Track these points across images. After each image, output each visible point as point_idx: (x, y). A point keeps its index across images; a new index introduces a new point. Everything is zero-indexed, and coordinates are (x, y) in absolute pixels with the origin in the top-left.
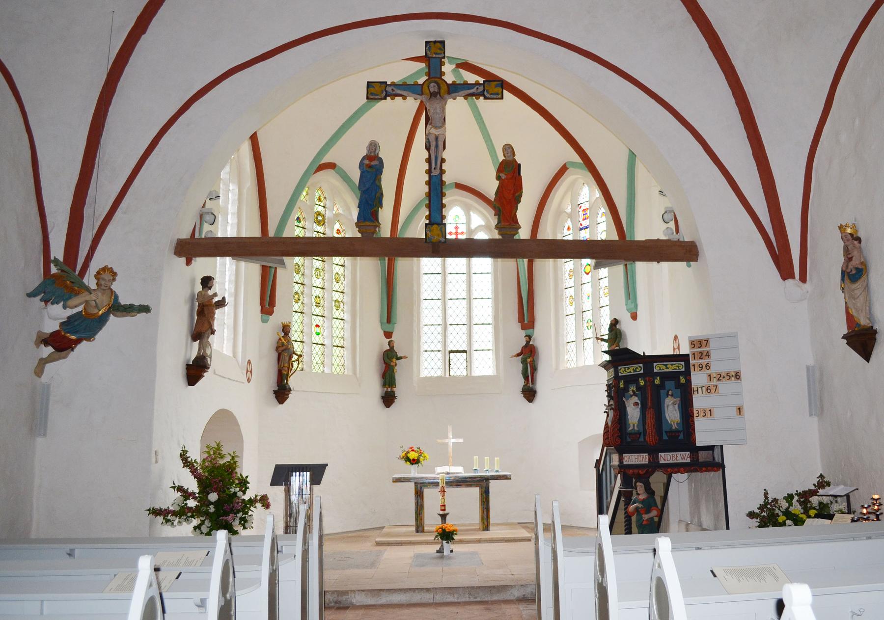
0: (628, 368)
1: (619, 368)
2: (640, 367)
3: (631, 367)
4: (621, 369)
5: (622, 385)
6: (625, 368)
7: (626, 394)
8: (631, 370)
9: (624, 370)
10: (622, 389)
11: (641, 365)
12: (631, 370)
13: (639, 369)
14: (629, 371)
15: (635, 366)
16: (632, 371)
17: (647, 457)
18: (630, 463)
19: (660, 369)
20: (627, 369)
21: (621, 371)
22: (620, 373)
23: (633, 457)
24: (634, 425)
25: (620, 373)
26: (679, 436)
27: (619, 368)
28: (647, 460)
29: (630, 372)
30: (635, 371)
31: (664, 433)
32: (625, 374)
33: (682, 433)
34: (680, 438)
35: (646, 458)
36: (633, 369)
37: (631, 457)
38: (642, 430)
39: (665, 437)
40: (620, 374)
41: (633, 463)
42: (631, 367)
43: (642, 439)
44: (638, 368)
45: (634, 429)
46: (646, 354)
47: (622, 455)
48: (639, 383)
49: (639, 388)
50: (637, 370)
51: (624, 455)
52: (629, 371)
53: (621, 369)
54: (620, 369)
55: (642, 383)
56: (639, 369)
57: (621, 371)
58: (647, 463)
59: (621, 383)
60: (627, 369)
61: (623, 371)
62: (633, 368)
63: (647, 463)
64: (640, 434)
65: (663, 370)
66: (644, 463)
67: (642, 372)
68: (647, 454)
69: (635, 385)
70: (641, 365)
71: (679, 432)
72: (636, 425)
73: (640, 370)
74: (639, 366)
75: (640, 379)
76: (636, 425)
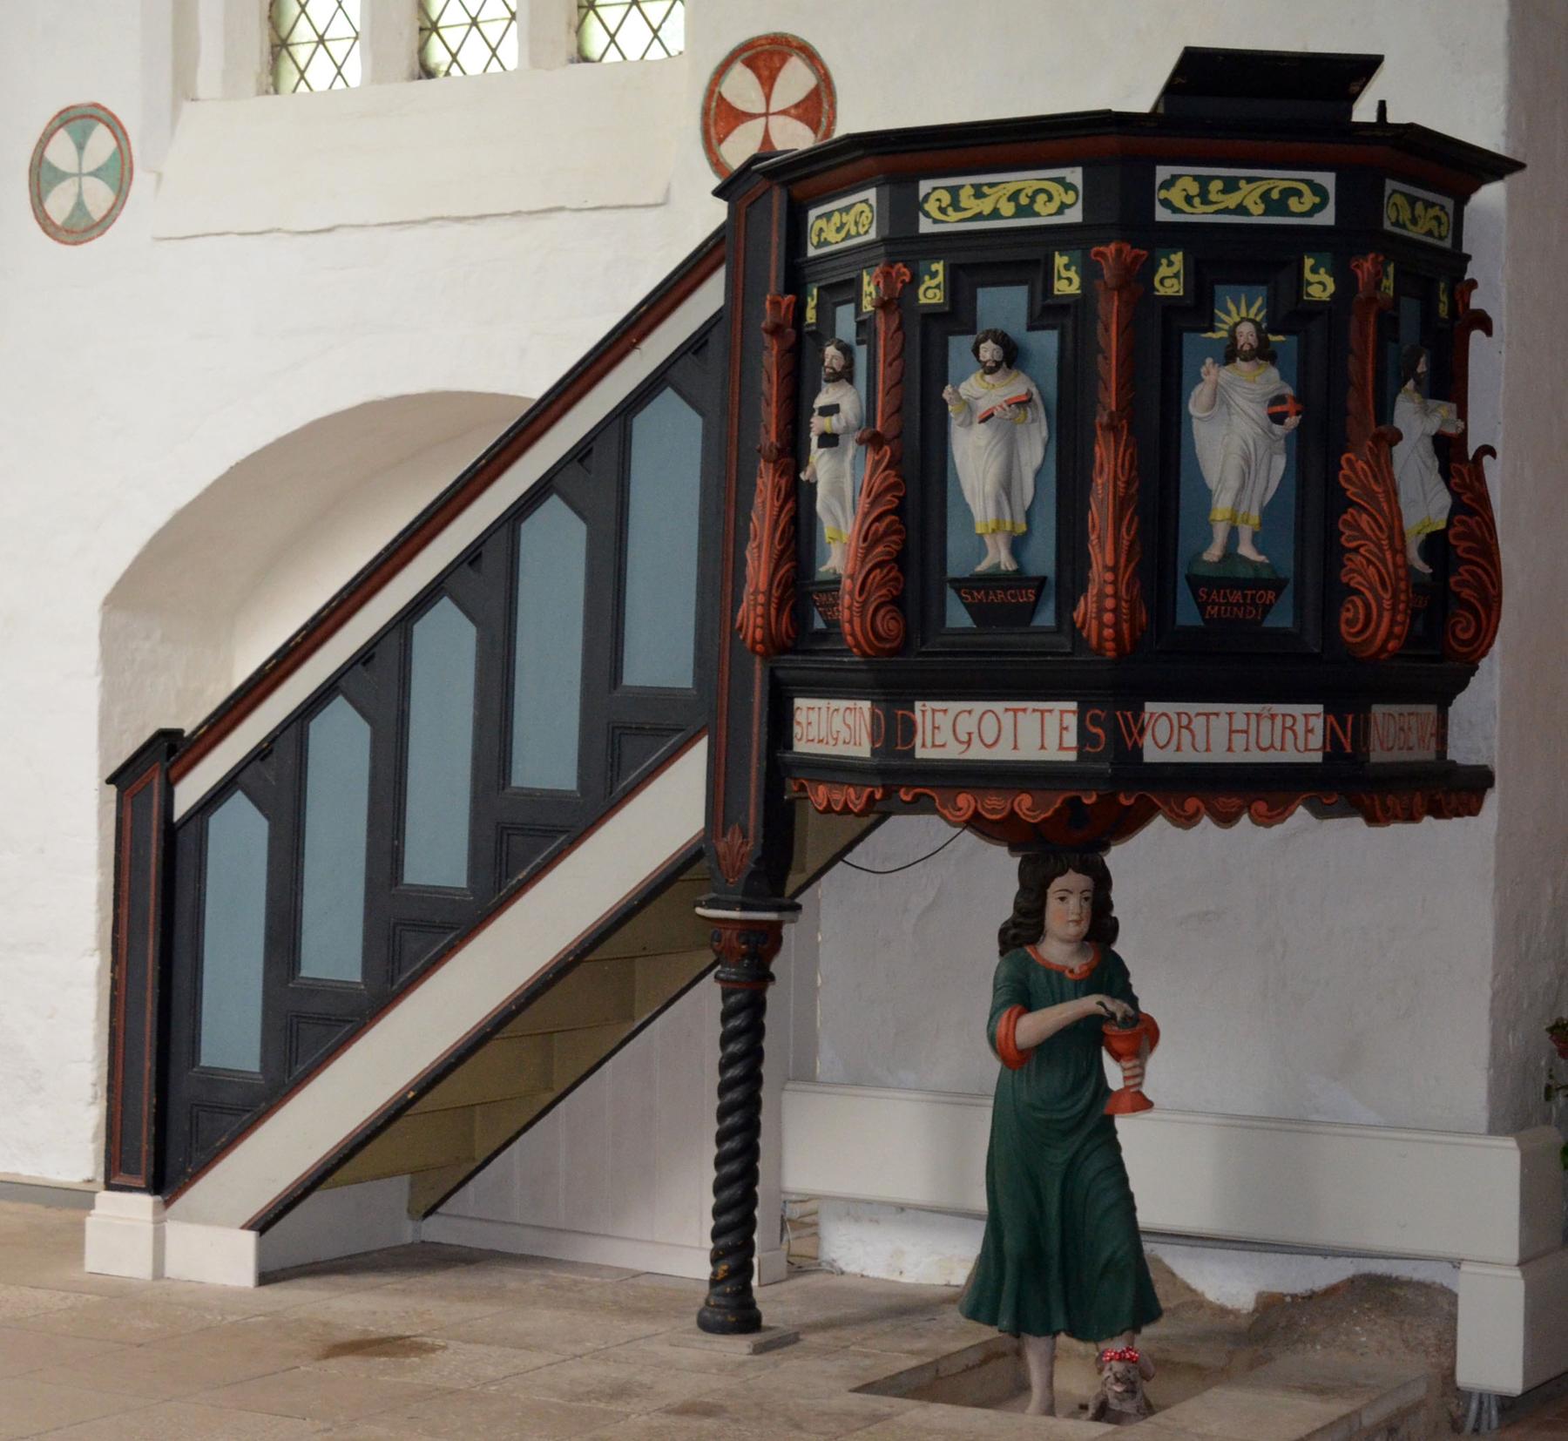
0: (1231, 186)
1: (1163, 173)
2: (1318, 189)
3: (1250, 180)
4: (1175, 178)
5: (931, 292)
6: (1204, 182)
7: (1187, 337)
8: (1250, 196)
9: (946, 198)
10: (1170, 303)
11: (1327, 180)
12: (1250, 196)
13: (1309, 199)
14: (1232, 200)
15: (1279, 179)
16: (1007, 208)
17: (1318, 724)
18: (1188, 756)
19: (1397, 224)
20: (1216, 186)
21: (1176, 196)
22: (1166, 203)
23: (1220, 726)
24: (1233, 535)
25: (1166, 203)
26: (1033, 609)
27: (1163, 173)
28: (1317, 740)
29: (1241, 209)
30: (1275, 205)
31: (1182, 584)
32: (1200, 215)
33: (1288, 592)
34: (1271, 622)
35: (1309, 731)
36: (1265, 197)
37: (1199, 724)
38: (1043, 559)
39: (1187, 614)
40: (1162, 215)
41: (1218, 755)
42: (1250, 180)
43: (1046, 617)
44: (1299, 194)
45: (1230, 552)
46: (1393, 118)
47: (1142, 709)
48: (1300, 283)
49: (1047, 311)
50: (1293, 204)
51: (1150, 707)
52: (1232, 200)
53: (1175, 178)
54: (1168, 184)
55: (1320, 285)
56: (1309, 199)
57: (1176, 196)
58: (1317, 757)
59: (1163, 271)
60: (1216, 186)
61: (1189, 199)
62: (1265, 186)
63: (1317, 757)
64: (1277, 586)
65: (1404, 226)
66: (1291, 756)
67: (1327, 217)
68: (1319, 708)
69: (1263, 289)
70: (1327, 180)
71: (1263, 584)
72: (1245, 534)
73: (1316, 209)
74: (1309, 183)
75: (1309, 262)
76: (1245, 534)
